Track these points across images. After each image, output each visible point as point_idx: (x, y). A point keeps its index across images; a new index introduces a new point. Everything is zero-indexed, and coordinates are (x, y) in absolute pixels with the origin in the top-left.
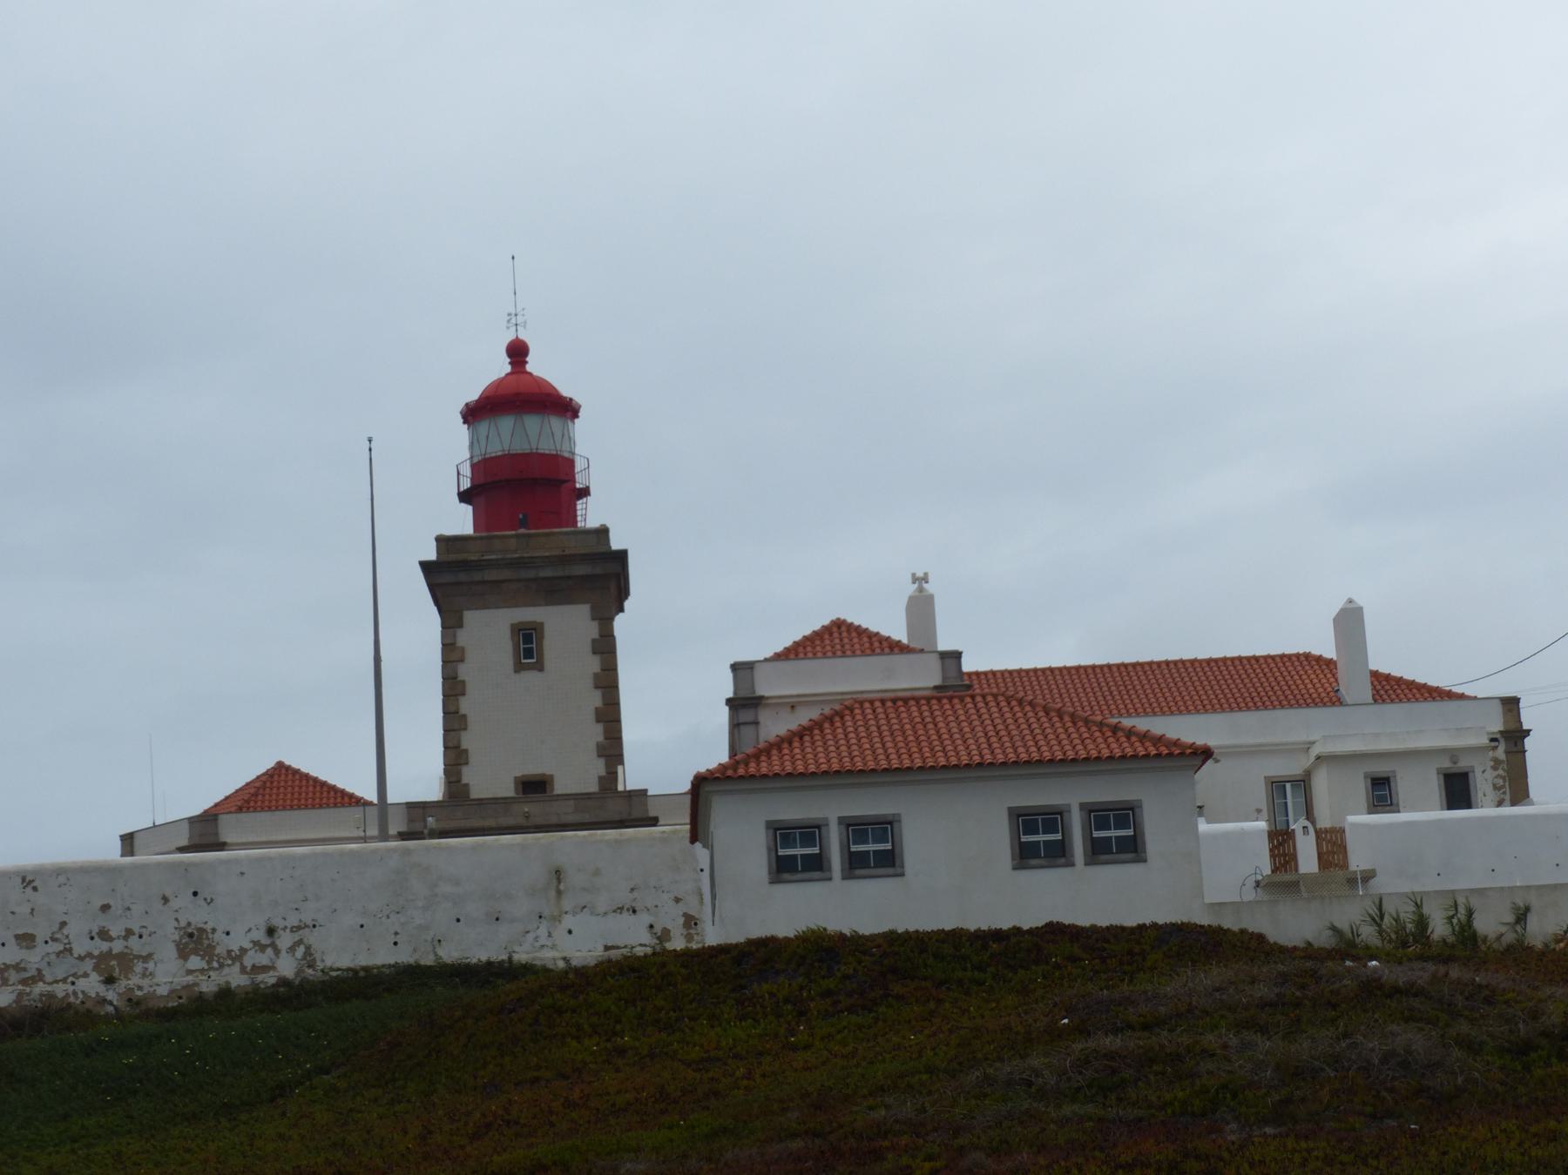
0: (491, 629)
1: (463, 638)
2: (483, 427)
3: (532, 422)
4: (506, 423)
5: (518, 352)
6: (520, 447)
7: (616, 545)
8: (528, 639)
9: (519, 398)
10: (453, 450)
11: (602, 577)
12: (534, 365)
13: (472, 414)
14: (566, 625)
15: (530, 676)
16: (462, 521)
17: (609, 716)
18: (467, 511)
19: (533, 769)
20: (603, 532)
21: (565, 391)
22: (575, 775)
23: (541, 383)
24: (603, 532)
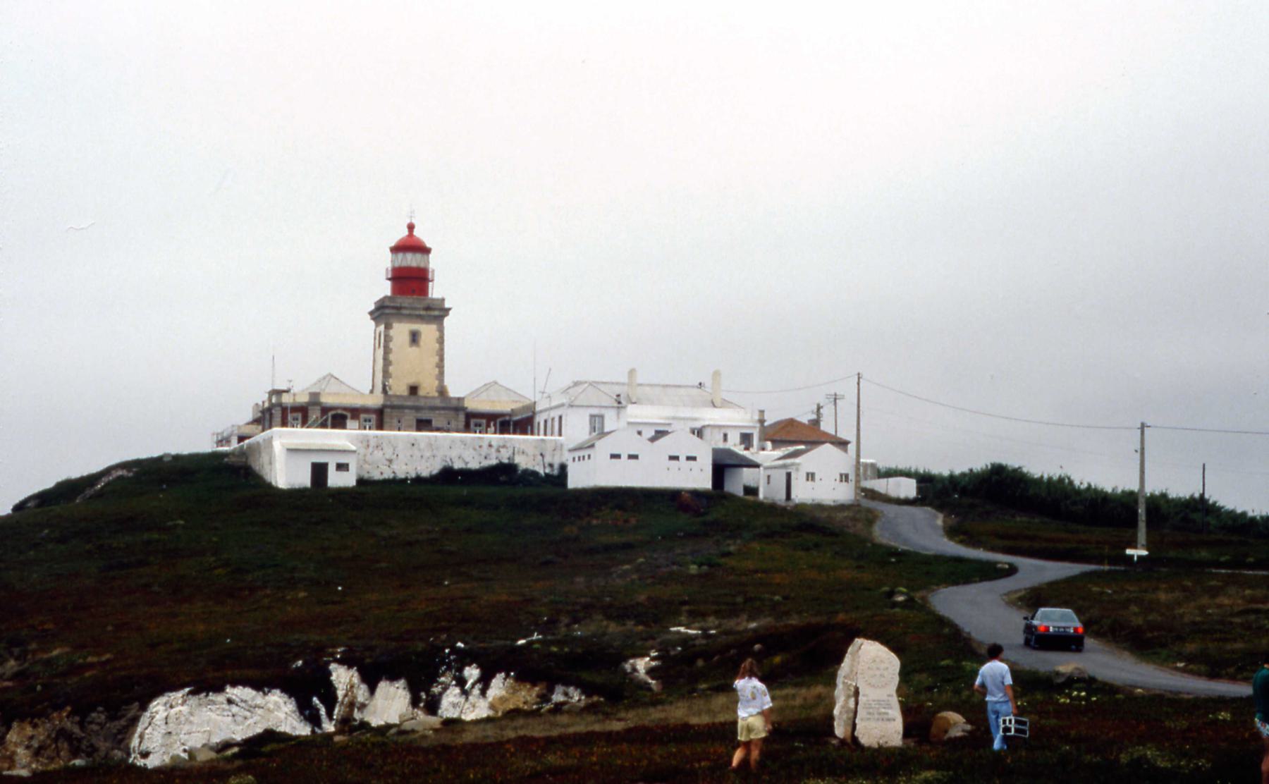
0: (401, 330)
1: (392, 332)
2: (400, 255)
3: (419, 256)
4: (409, 256)
5: (411, 227)
6: (414, 264)
7: (447, 305)
8: (415, 338)
9: (412, 245)
10: (386, 262)
11: (437, 313)
12: (416, 233)
13: (396, 249)
14: (428, 331)
15: (414, 349)
16: (385, 289)
17: (440, 365)
18: (389, 283)
19: (412, 380)
20: (443, 300)
21: (428, 245)
22: (428, 388)
23: (418, 240)
24: (443, 300)
